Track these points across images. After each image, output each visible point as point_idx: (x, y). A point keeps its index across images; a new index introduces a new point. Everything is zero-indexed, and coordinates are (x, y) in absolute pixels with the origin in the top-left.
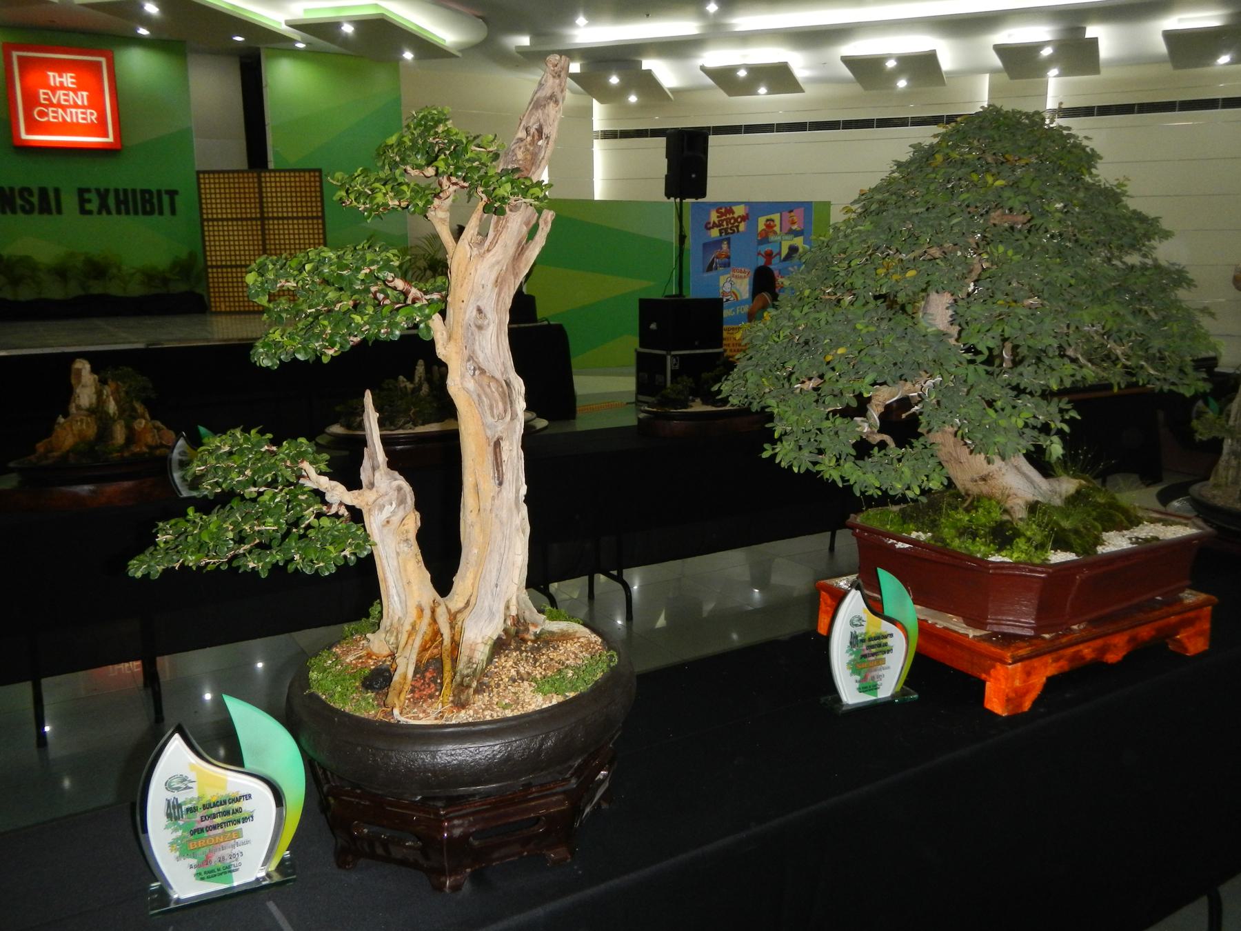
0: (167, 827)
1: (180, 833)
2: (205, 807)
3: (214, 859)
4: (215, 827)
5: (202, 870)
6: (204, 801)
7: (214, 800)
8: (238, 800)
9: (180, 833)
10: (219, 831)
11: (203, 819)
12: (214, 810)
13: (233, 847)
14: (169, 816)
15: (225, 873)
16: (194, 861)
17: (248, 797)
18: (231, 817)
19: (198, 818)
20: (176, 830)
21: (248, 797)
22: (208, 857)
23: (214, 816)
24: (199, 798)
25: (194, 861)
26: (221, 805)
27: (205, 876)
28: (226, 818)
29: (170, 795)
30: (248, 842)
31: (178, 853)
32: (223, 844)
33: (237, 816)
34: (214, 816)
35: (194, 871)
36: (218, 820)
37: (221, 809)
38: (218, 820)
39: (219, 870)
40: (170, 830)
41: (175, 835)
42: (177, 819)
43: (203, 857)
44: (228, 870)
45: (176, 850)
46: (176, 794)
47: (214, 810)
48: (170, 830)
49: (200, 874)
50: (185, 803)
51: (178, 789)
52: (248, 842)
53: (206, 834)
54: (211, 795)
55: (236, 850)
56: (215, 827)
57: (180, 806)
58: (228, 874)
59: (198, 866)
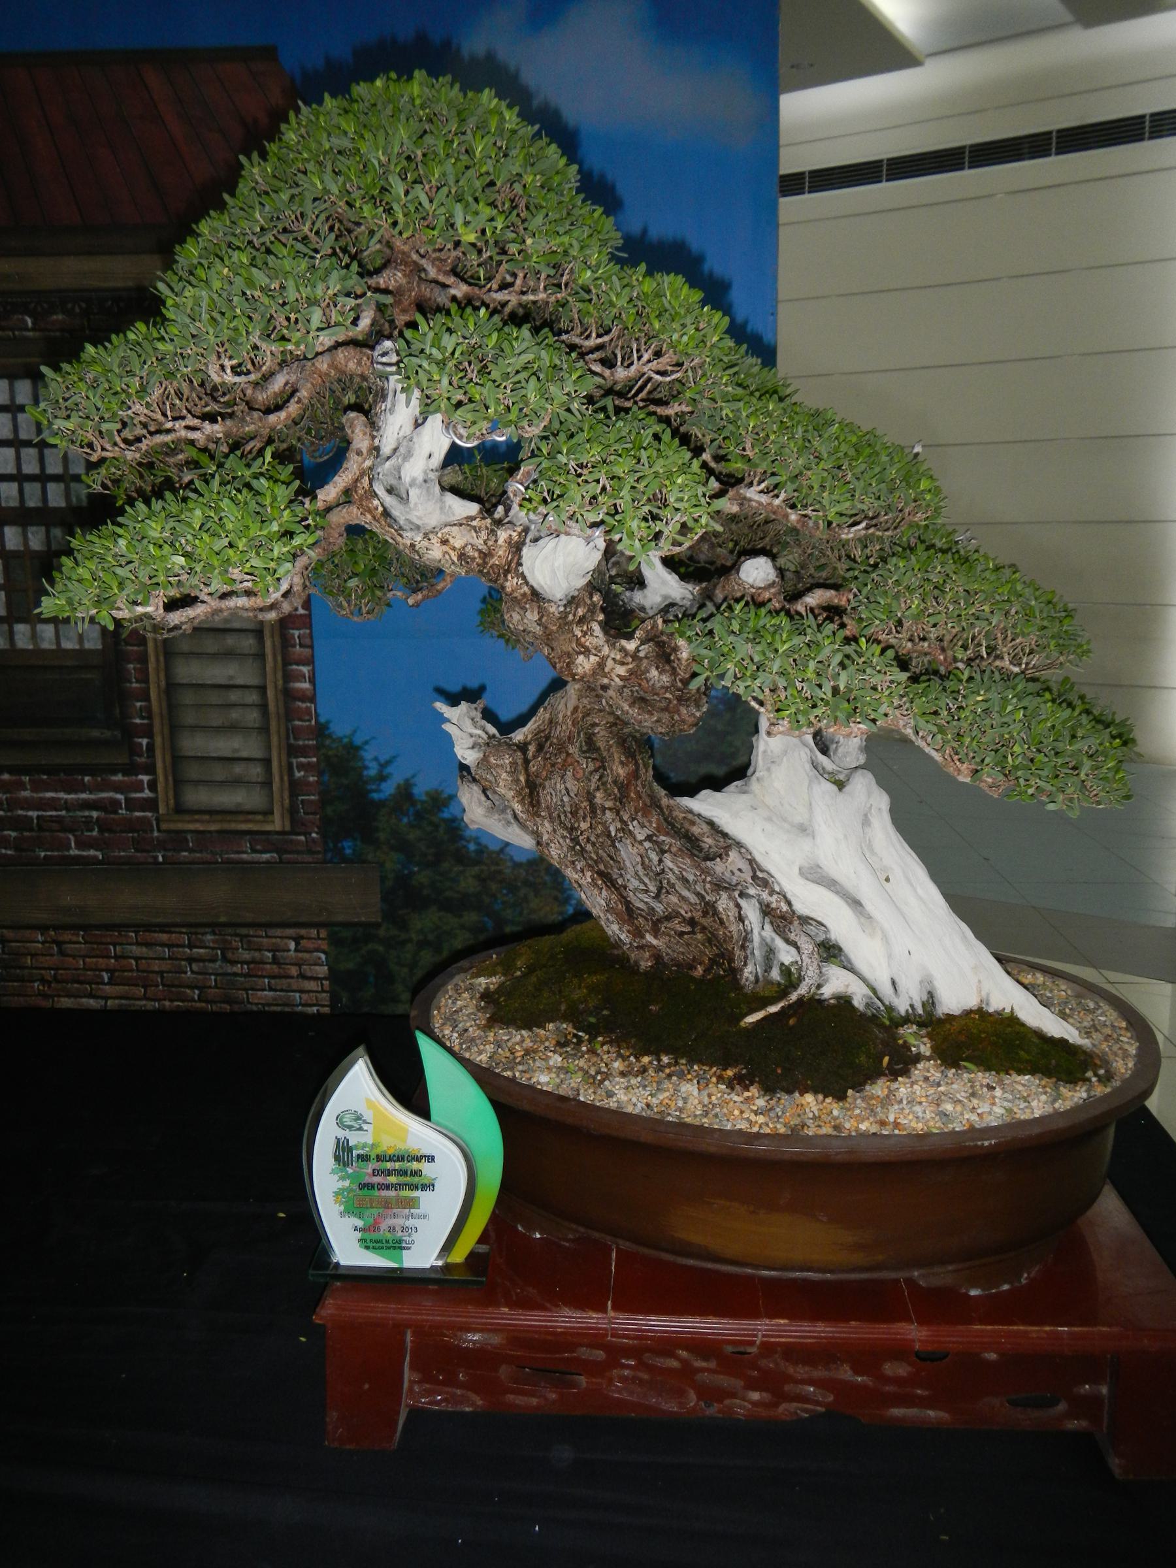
0: (333, 1172)
1: (347, 1183)
2: (379, 1158)
3: (384, 1226)
4: (388, 1187)
5: (368, 1236)
6: (379, 1151)
7: (391, 1152)
8: (419, 1159)
9: (347, 1183)
10: (392, 1193)
11: (376, 1173)
12: (389, 1165)
13: (407, 1218)
14: (337, 1158)
15: (395, 1248)
16: (360, 1223)
17: (431, 1159)
18: (408, 1179)
19: (370, 1171)
20: (342, 1178)
21: (431, 1159)
22: (376, 1222)
23: (388, 1173)
24: (373, 1145)
25: (360, 1223)
26: (398, 1160)
27: (371, 1245)
28: (402, 1179)
29: (341, 1134)
30: (425, 1217)
31: (342, 1208)
32: (395, 1211)
33: (416, 1180)
34: (388, 1173)
35: (359, 1235)
36: (392, 1179)
37: (397, 1165)
38: (392, 1179)
39: (387, 1242)
40: (336, 1177)
41: (341, 1184)
42: (346, 1165)
43: (371, 1221)
44: (398, 1246)
45: (341, 1203)
46: (347, 1133)
47: (389, 1165)
48: (336, 1177)
49: (365, 1240)
50: (356, 1147)
51: (350, 1127)
52: (425, 1217)
53: (376, 1193)
54: (388, 1144)
55: (410, 1223)
56: (388, 1187)
57: (350, 1149)
58: (397, 1251)
59: (362, 1230)
